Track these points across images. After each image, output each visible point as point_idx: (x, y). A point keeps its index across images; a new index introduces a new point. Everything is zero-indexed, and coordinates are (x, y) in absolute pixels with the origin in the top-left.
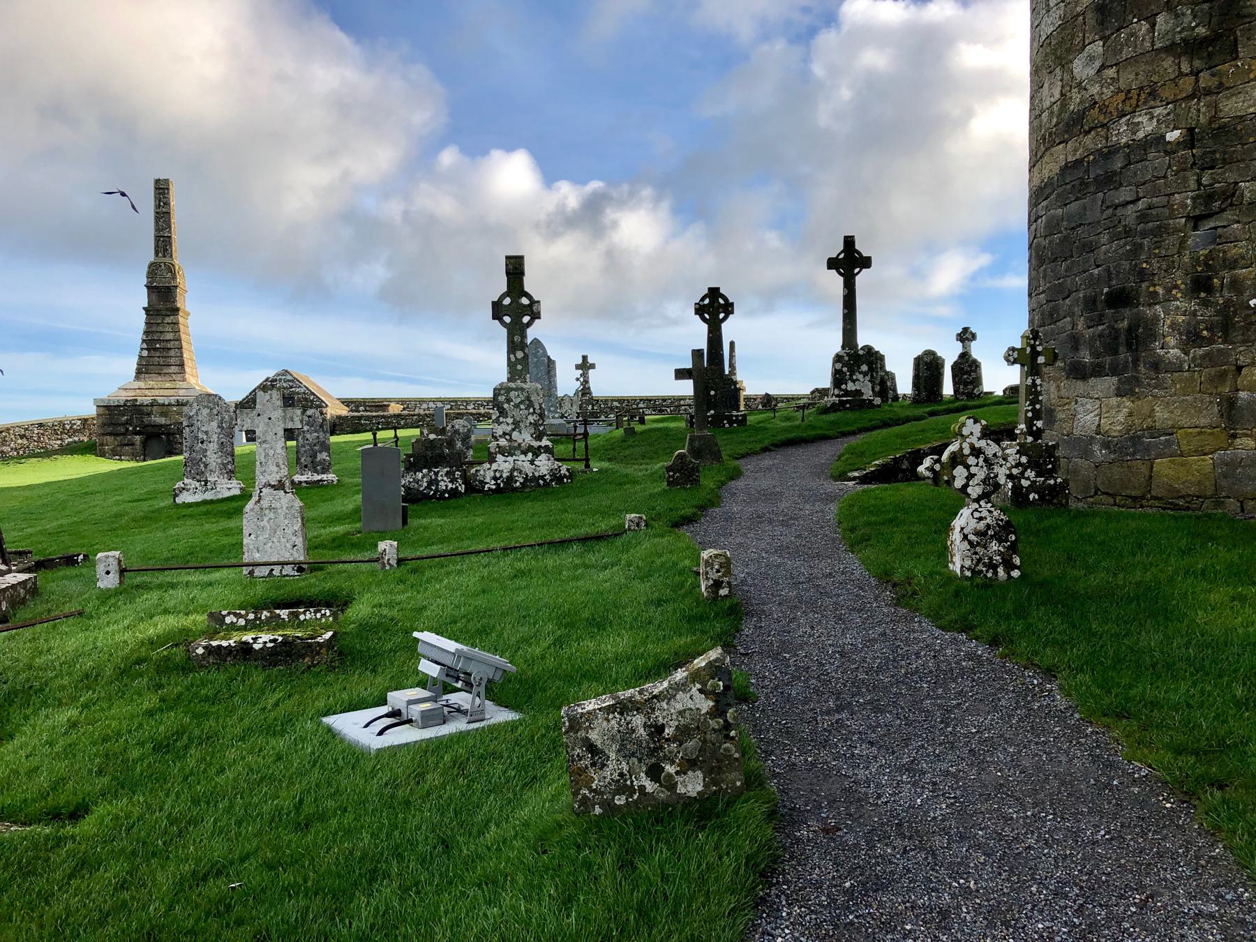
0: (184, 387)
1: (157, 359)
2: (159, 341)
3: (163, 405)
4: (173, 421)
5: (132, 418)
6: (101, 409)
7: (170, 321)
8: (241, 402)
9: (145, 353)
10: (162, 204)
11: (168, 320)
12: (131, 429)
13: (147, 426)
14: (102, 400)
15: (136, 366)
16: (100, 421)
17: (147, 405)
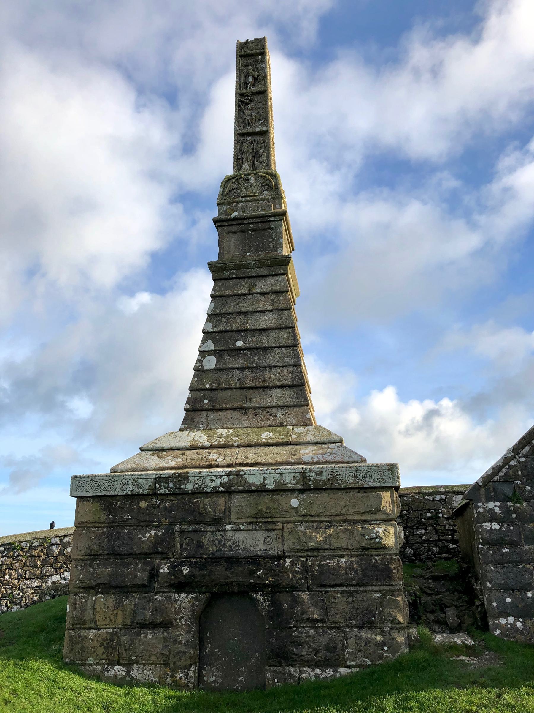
0: (309, 438)
1: (237, 374)
2: (242, 332)
3: (261, 490)
4: (290, 544)
5: (170, 533)
6: (89, 506)
7: (267, 289)
8: (488, 479)
9: (211, 362)
10: (251, 79)
11: (263, 286)
12: (164, 570)
13: (215, 560)
14: (93, 478)
15: (187, 394)
16: (83, 545)
17: (215, 492)
